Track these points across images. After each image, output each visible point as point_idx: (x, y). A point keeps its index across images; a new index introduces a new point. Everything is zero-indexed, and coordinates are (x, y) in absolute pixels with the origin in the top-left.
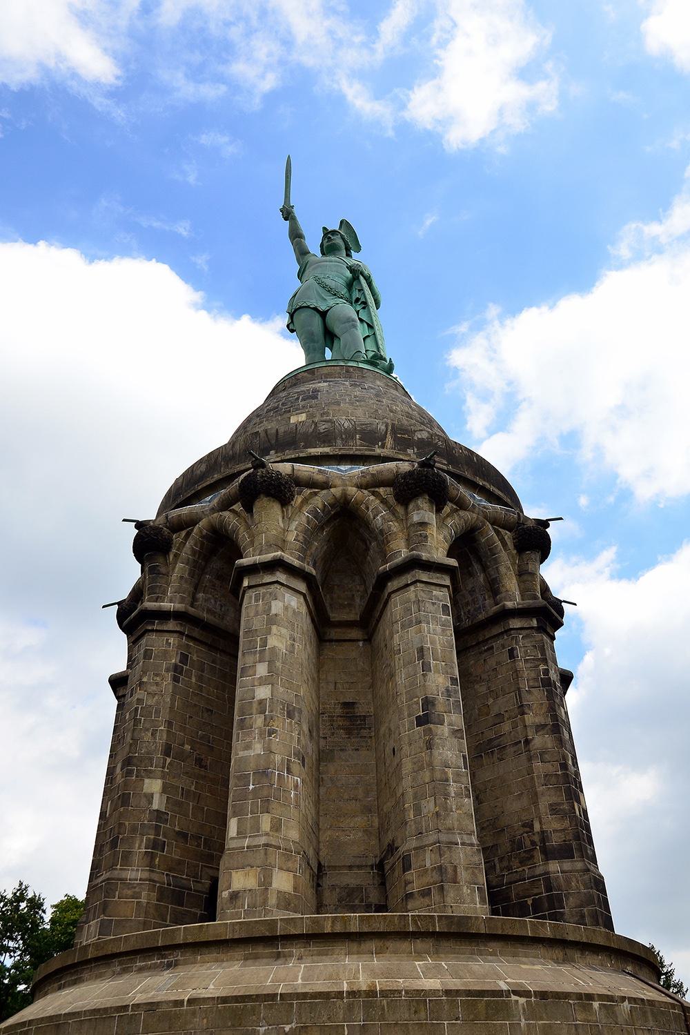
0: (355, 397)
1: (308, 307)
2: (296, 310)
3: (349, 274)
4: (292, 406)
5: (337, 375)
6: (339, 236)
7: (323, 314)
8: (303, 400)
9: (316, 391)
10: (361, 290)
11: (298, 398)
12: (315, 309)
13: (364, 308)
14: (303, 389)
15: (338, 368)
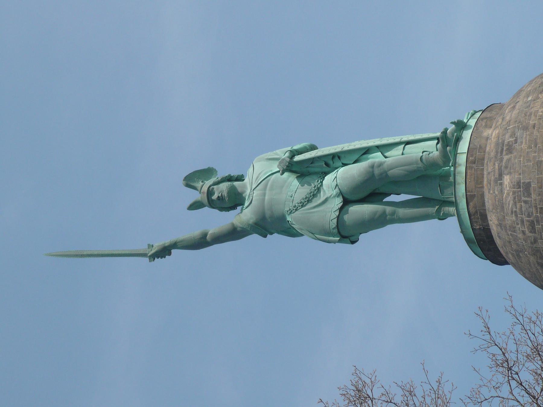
0: (530, 147)
1: (338, 217)
2: (339, 232)
3: (286, 174)
4: (536, 207)
5: (479, 172)
6: (215, 187)
7: (347, 202)
8: (529, 195)
9: (518, 185)
10: (312, 160)
11: (526, 202)
12: (341, 209)
13: (339, 158)
14: (510, 199)
15: (468, 172)
